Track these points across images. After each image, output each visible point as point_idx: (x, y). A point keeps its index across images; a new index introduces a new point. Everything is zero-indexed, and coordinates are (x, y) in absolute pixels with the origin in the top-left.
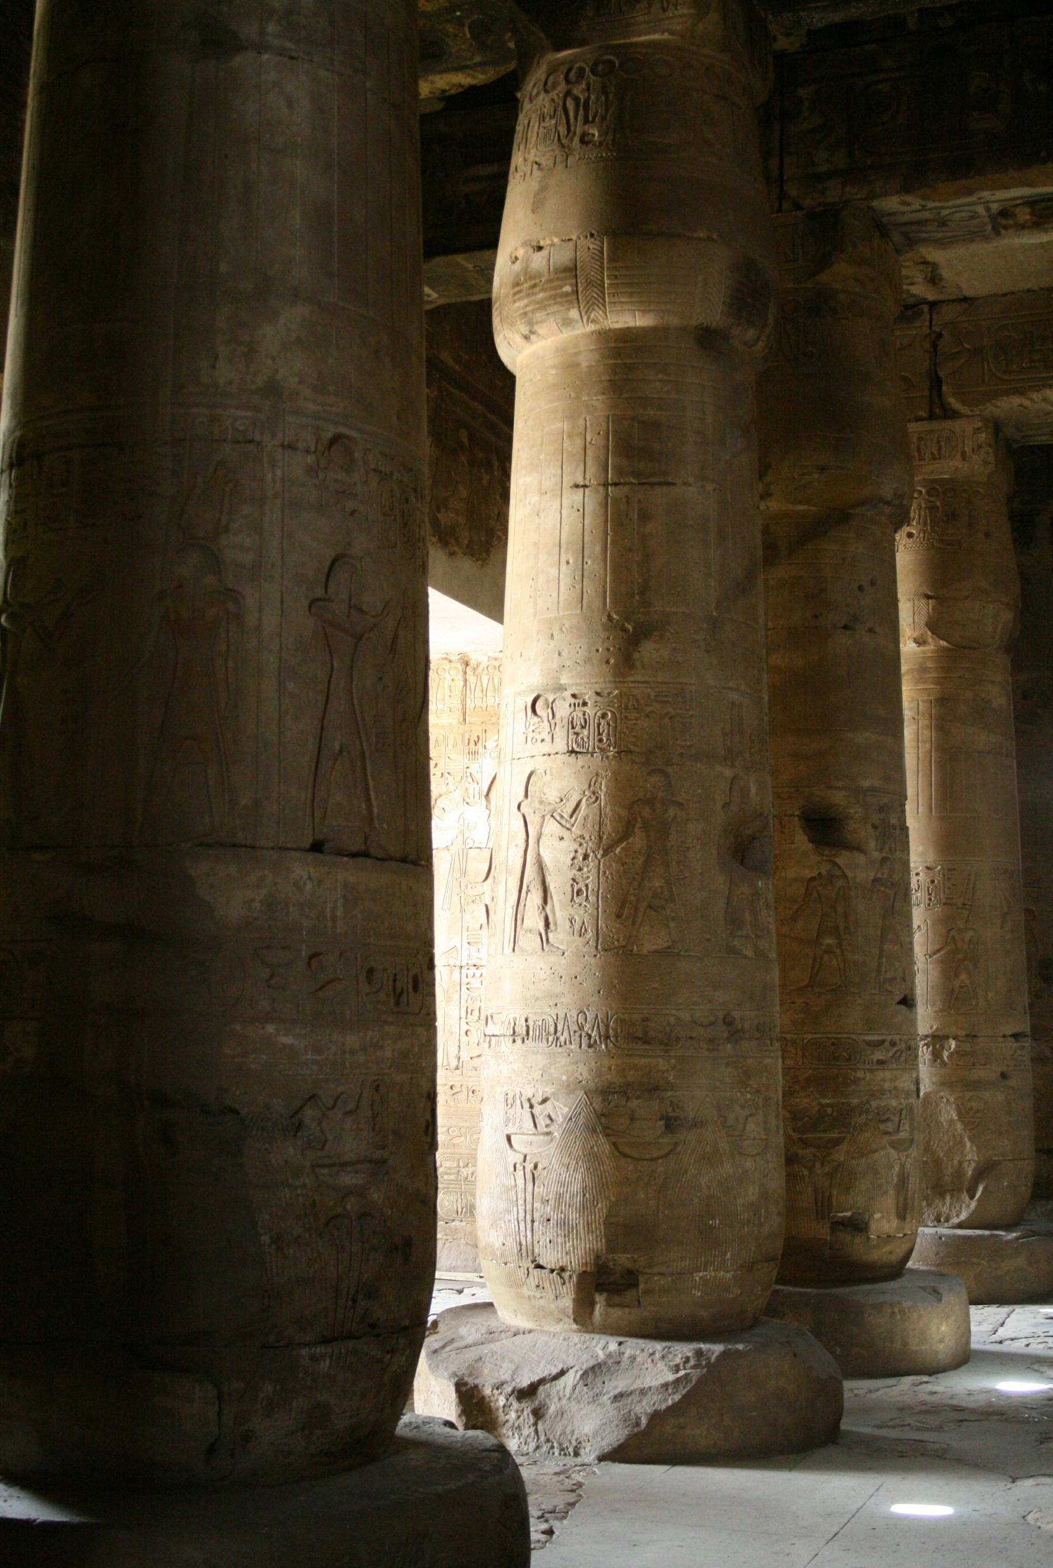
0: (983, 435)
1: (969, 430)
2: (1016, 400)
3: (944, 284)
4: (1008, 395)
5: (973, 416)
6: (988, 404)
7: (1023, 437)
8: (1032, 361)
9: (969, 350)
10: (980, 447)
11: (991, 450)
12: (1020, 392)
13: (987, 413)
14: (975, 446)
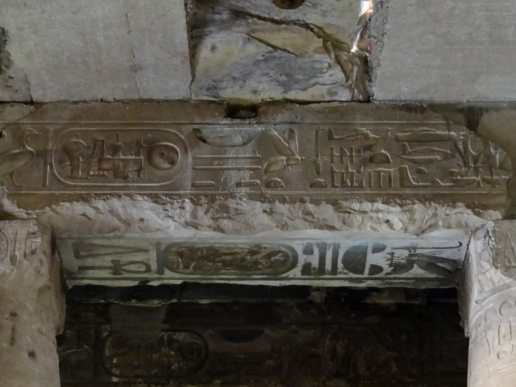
0: (39, 240)
1: (22, 233)
2: (79, 208)
3: (10, 72)
4: (70, 201)
5: (28, 219)
6: (47, 209)
7: (82, 268)
8: (100, 169)
9: (31, 153)
10: (33, 252)
11: (45, 260)
12: (84, 199)
13: (44, 219)
14: (28, 252)
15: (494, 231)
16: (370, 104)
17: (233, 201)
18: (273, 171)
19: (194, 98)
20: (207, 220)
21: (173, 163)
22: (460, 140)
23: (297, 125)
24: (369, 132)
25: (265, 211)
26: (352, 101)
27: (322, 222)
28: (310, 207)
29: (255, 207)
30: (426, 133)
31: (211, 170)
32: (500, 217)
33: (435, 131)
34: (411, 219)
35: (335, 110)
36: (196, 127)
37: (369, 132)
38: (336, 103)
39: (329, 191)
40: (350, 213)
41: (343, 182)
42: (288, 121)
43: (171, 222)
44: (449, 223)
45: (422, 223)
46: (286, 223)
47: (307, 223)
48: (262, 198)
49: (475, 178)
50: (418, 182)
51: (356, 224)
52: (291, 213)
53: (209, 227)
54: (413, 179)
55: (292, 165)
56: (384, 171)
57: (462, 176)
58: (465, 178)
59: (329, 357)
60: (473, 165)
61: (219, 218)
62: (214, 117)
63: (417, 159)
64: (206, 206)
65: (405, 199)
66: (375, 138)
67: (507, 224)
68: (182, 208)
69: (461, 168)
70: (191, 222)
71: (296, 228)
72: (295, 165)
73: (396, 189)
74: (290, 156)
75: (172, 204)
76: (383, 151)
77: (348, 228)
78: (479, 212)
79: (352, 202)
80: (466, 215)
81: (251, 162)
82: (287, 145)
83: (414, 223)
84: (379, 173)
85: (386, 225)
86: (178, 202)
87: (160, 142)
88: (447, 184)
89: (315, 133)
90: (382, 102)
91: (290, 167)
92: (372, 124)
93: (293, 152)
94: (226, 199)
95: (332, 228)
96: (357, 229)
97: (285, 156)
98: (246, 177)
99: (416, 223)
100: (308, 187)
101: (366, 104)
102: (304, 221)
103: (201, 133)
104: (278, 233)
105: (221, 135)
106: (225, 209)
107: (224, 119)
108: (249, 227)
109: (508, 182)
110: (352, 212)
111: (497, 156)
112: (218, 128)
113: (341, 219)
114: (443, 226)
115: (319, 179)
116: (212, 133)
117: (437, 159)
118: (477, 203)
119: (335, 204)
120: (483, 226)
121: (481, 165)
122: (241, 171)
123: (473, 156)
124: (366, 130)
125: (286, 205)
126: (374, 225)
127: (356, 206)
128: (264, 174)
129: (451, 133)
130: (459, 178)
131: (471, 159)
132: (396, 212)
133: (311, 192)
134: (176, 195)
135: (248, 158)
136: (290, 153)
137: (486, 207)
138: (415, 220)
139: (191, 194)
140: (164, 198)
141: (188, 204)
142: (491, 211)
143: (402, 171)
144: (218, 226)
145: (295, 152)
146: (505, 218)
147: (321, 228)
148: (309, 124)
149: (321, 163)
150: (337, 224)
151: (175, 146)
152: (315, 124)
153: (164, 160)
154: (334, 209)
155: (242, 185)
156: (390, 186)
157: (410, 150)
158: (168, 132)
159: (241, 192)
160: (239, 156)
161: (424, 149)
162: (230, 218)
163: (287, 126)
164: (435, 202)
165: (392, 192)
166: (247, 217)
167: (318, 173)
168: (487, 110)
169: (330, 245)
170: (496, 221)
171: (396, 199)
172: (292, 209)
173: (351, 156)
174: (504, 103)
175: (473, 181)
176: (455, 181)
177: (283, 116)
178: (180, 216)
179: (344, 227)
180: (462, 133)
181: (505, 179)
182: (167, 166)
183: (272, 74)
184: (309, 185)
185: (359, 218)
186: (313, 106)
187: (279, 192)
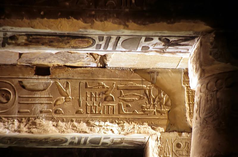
15: (160, 138)
16: (106, 69)
17: (38, 120)
18: (58, 105)
19: (19, 64)
20: (25, 129)
21: (8, 99)
22: (147, 89)
24: (104, 84)
25: (54, 125)
26: (97, 67)
27: (80, 130)
28: (76, 124)
29: (49, 123)
30: (131, 85)
31: (28, 104)
32: (164, 131)
34: (122, 129)
35: (89, 72)
36: (20, 80)
37: (104, 84)
38: (89, 68)
39: (85, 115)
40: (94, 126)
41: (91, 111)
42: (66, 78)
43: (7, 130)
44: (140, 132)
45: (128, 131)
46: (64, 131)
47: (74, 131)
48: (52, 119)
50: (126, 112)
51: (97, 131)
52: (66, 126)
53: (26, 132)
54: (124, 110)
56: (111, 106)
57: (147, 109)
58: (148, 110)
59: (77, 154)
60: (153, 103)
61: (31, 128)
62: (29, 74)
64: (25, 123)
65: (120, 121)
67: (167, 134)
68: (13, 124)
70: (17, 130)
71: (68, 132)
72: (69, 101)
73: (116, 115)
74: (66, 97)
75: (8, 122)
77: (93, 133)
78: (154, 127)
79: (95, 121)
80: (148, 129)
81: (47, 100)
82: (65, 91)
83: (124, 131)
84: (108, 106)
85: (111, 131)
86: (11, 121)
87: (1, 88)
88: (140, 113)
89: (79, 84)
90: (111, 68)
91: (66, 103)
92: (106, 80)
93: (68, 94)
94: (35, 119)
95: (86, 132)
96: (97, 133)
97: (64, 96)
98: (45, 108)
99: (125, 131)
100: (75, 114)
101: (103, 69)
102: (72, 130)
103: (22, 83)
104: (60, 134)
105: (33, 84)
106: (34, 124)
107: (34, 76)
108: (45, 131)
109: (168, 112)
110: (95, 126)
111: (164, 99)
112: (31, 81)
113: (90, 129)
114: (137, 133)
116: (28, 83)
118: (153, 123)
119: (88, 123)
120: (155, 134)
122: (43, 105)
124: (103, 83)
125: (64, 123)
126: (105, 131)
127: (97, 123)
128: (54, 106)
129: (143, 85)
130: (146, 109)
131: (152, 100)
132: (116, 127)
133: (77, 116)
134: (10, 117)
135: (46, 97)
136: (66, 95)
137: (157, 126)
138: (124, 130)
139: (18, 117)
140: (4, 119)
141: (16, 123)
142: (159, 128)
143: (119, 105)
144: (30, 131)
145: (69, 94)
146: (166, 131)
147: (80, 132)
148: (76, 79)
150: (88, 131)
151: (9, 90)
152: (79, 79)
153: (4, 98)
154: (86, 125)
155: (43, 112)
156: (113, 114)
157: (123, 95)
158: (6, 83)
159: (42, 116)
160: (41, 96)
162: (36, 128)
163: (66, 80)
164: (134, 123)
165: (114, 117)
166: (45, 128)
167: (80, 106)
168: (162, 72)
169: (83, 137)
170: (161, 133)
171: (116, 121)
172: (67, 125)
173: (96, 97)
174: (170, 69)
176: (144, 111)
177: (63, 74)
178: (12, 127)
179: (91, 132)
180: (148, 86)
181: (167, 111)
182: (5, 101)
183: (59, 58)
185: (98, 128)
186: (78, 69)
187: (61, 116)
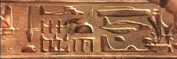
22: (154, 15)
23: (12, 4)
24: (75, 9)
33: (132, 8)
41: (51, 49)
49: (166, 45)
55: (6, 35)
57: (155, 43)
58: (158, 45)
60: (164, 35)
63: (116, 30)
66: (80, 14)
69: (154, 37)
76: (87, 24)
89: (28, 9)
115: (30, 46)
117: (133, 30)
121: (172, 35)
123: (165, 28)
130: (153, 44)
145: (9, 24)
149: (32, 32)
156: (92, 51)
161: (122, 22)
167: (29, 40)
173: (59, 28)
175: (165, 47)
184: (20, 50)
